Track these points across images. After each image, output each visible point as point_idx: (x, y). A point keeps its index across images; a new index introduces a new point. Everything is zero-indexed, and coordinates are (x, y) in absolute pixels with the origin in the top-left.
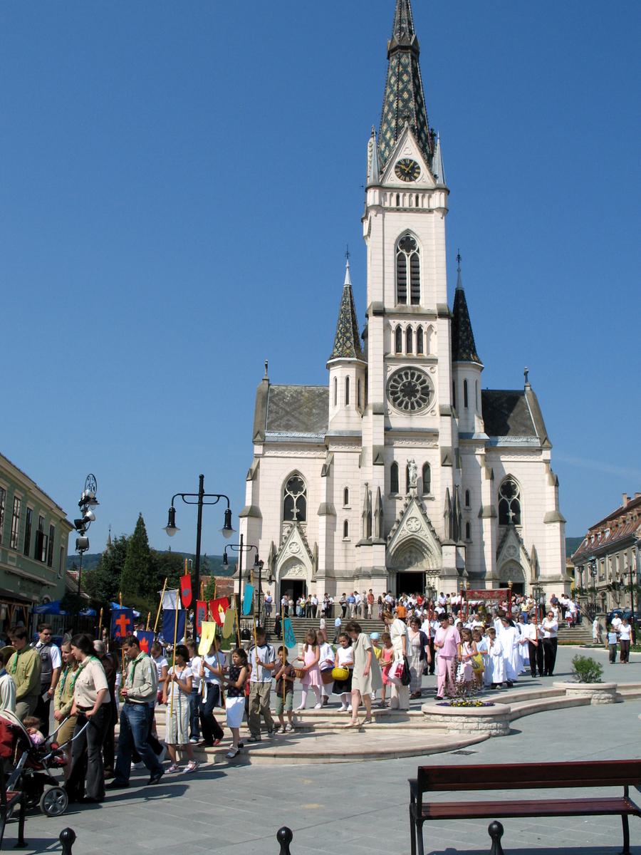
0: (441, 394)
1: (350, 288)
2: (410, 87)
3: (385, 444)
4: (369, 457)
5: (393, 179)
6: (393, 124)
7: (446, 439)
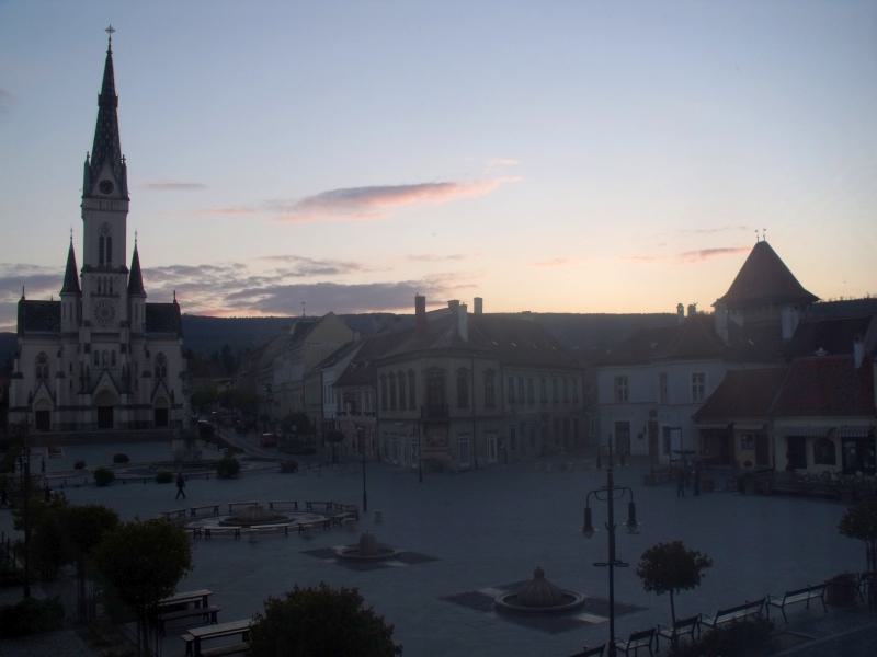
4: (83, 349)
7: (124, 339)
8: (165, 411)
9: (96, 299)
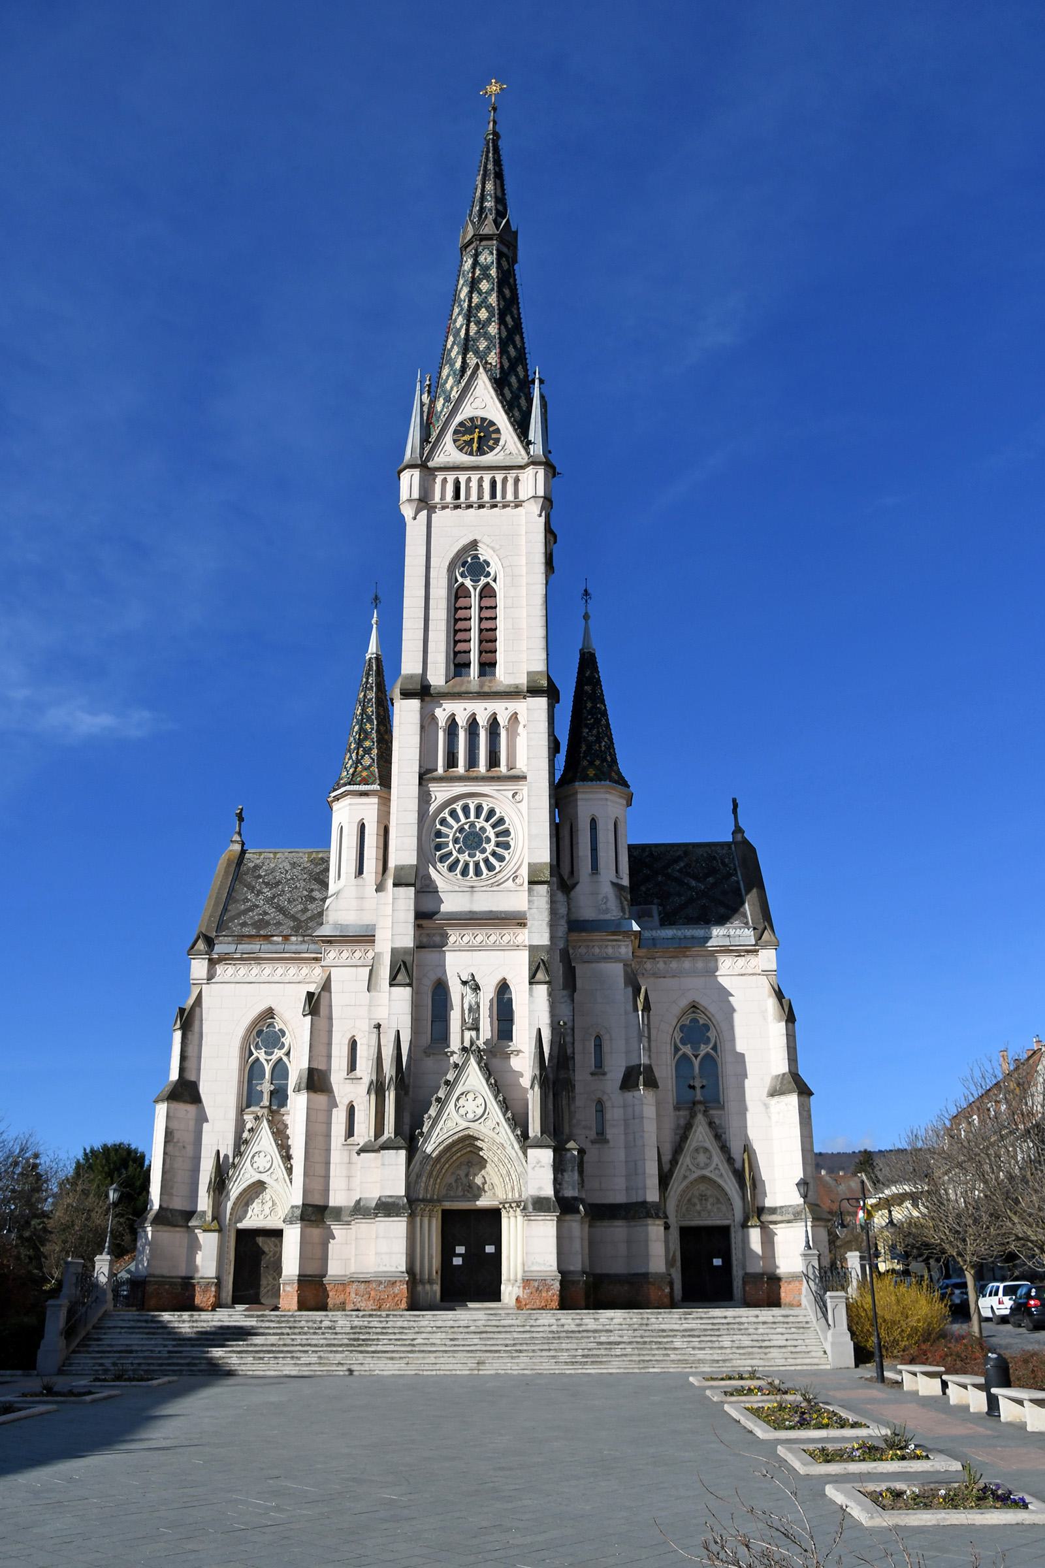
1: (377, 659)
2: (493, 300)
3: (420, 946)
4: (385, 972)
5: (448, 452)
6: (458, 365)
7: (538, 933)
8: (724, 1232)
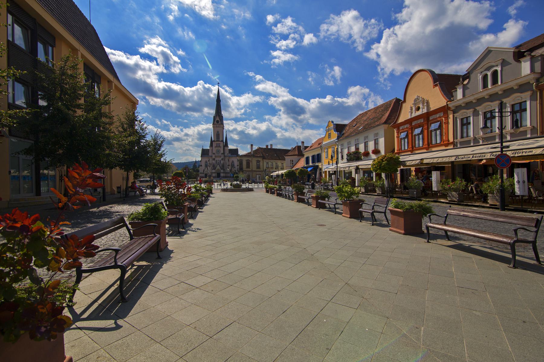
0: (222, 152)
9: (216, 148)
